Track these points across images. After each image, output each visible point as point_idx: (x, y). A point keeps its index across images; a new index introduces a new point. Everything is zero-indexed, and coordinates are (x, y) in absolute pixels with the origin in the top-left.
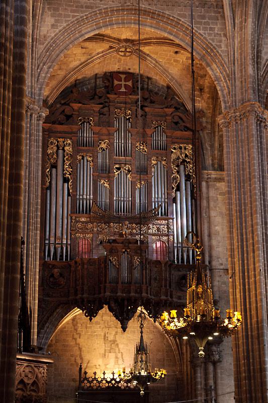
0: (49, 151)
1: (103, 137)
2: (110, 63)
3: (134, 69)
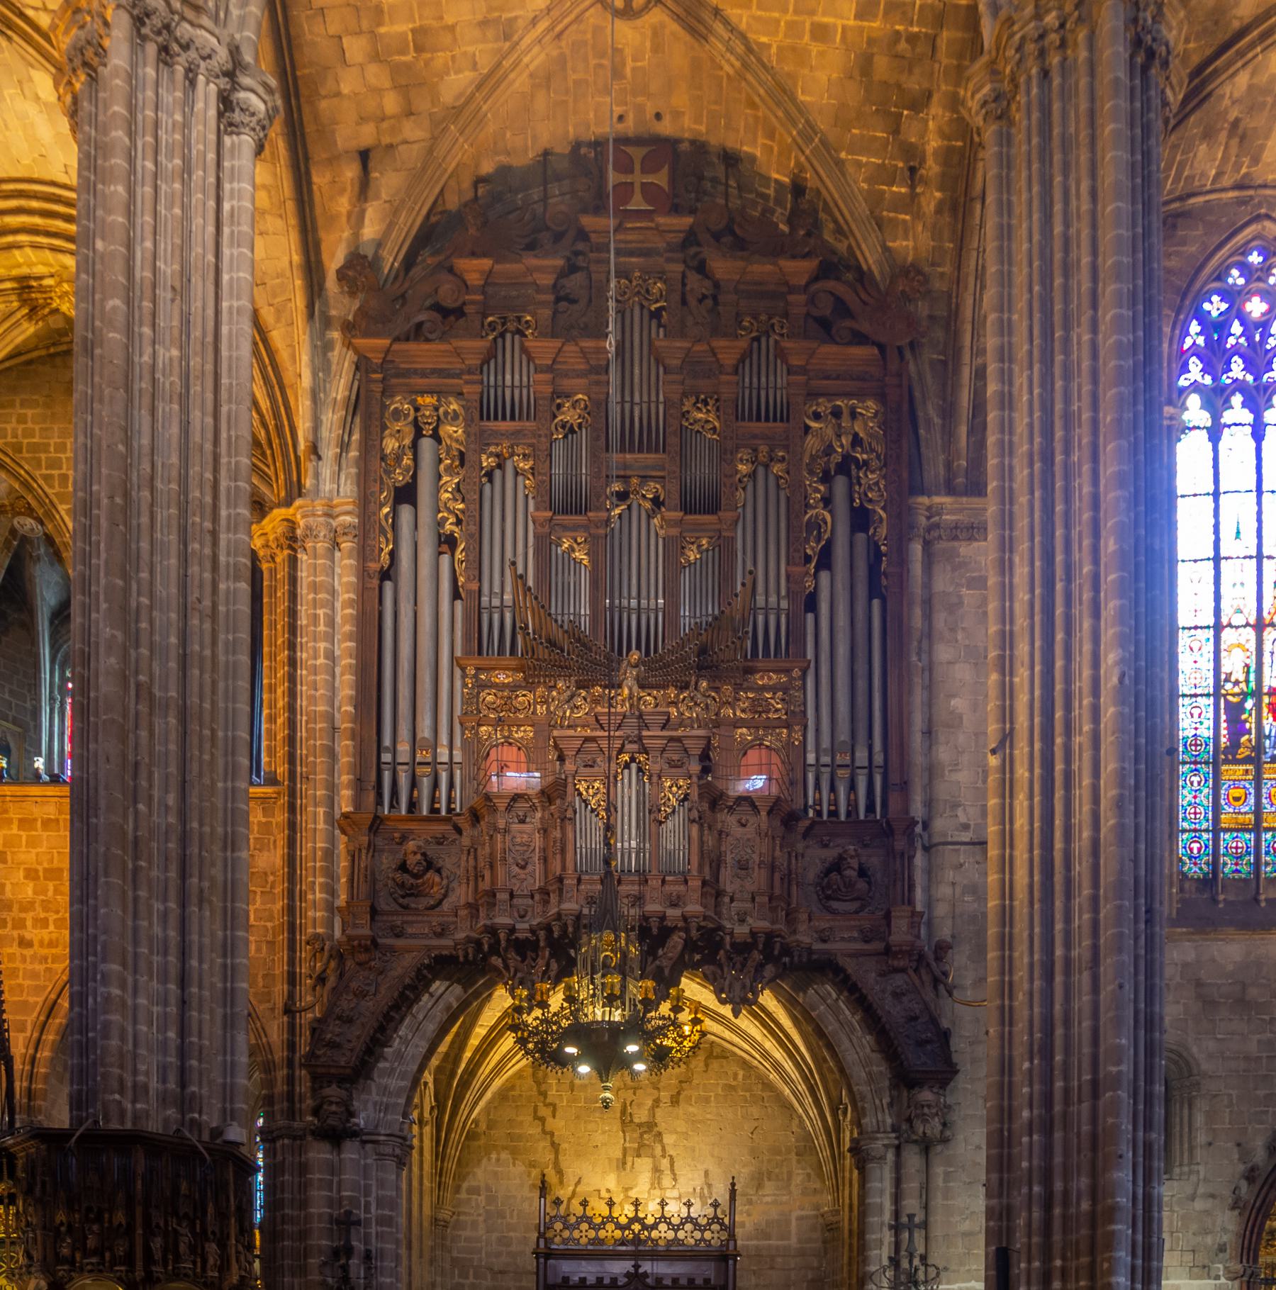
0: (390, 445)
1: (567, 384)
2: (586, 81)
3: (677, 115)
